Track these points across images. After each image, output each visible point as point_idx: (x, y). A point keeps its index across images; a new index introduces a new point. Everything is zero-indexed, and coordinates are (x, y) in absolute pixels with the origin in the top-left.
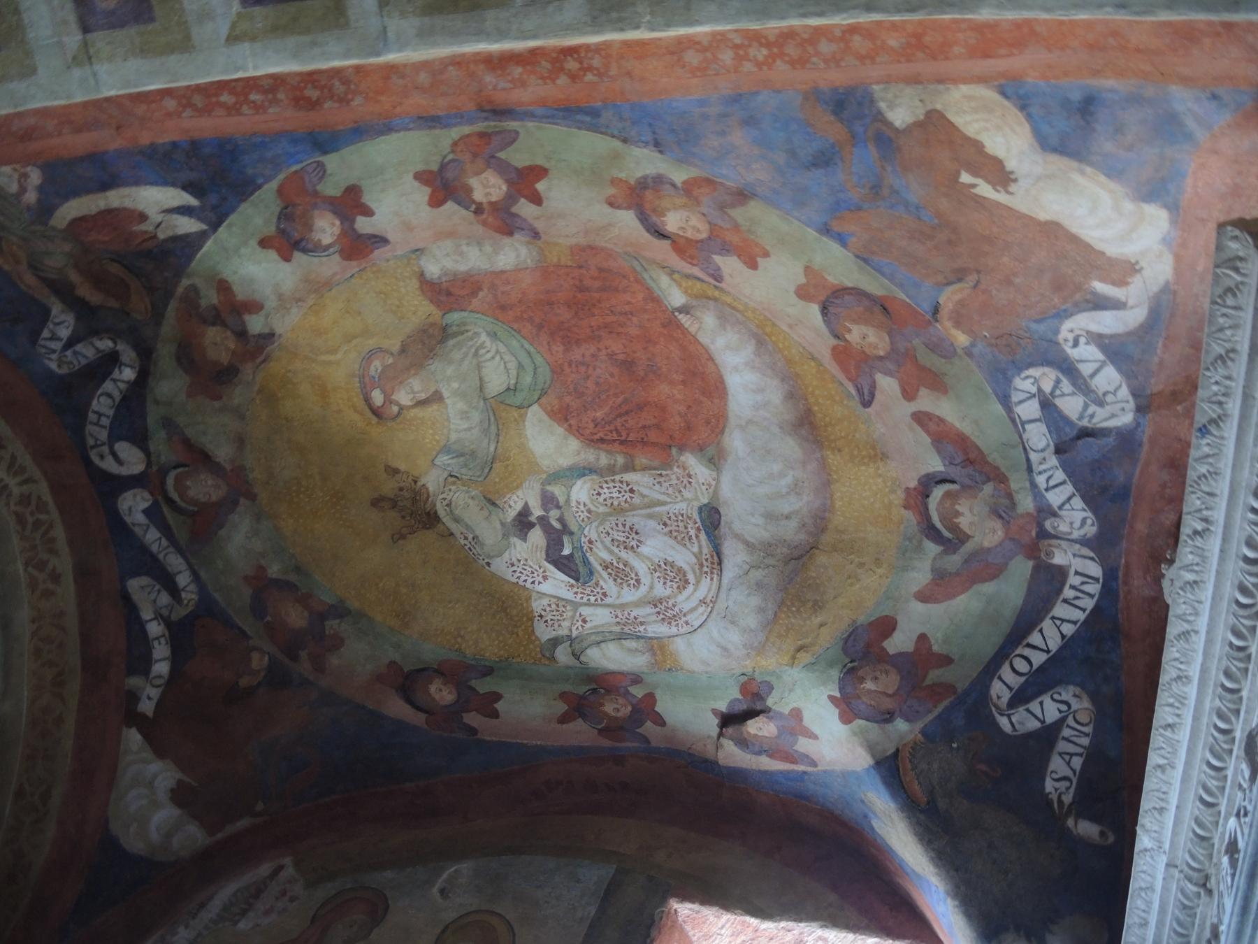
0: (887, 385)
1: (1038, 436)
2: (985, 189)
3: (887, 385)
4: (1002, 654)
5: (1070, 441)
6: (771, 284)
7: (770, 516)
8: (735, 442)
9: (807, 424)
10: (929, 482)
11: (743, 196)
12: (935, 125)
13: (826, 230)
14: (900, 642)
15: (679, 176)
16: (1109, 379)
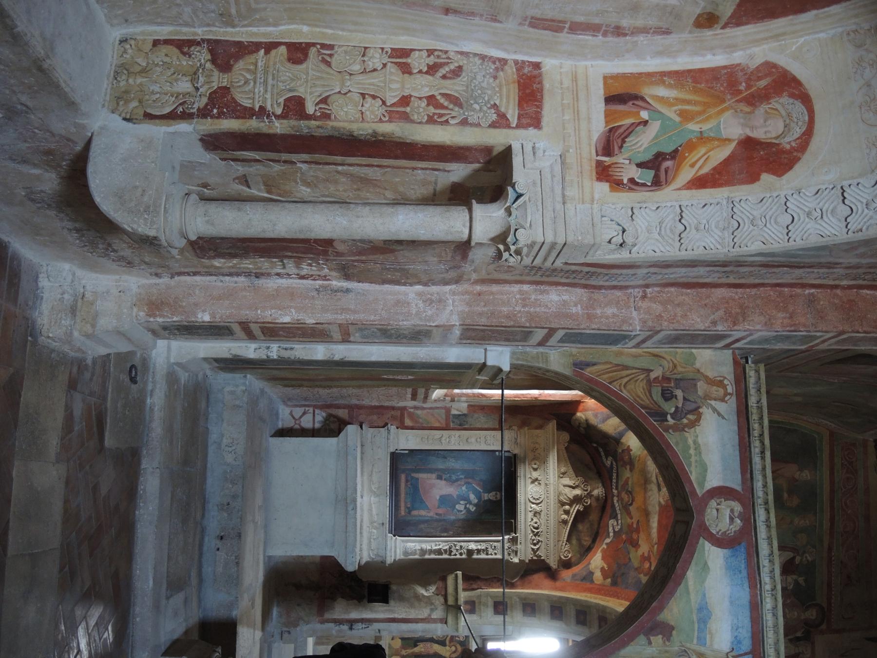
0: (635, 526)
1: (619, 516)
2: (605, 566)
3: (635, 526)
4: (617, 470)
5: (615, 517)
6: (644, 548)
7: (651, 490)
8: (657, 508)
9: (647, 514)
10: (631, 504)
11: (636, 569)
12: (605, 577)
13: (630, 559)
14: (628, 467)
15: (642, 575)
16: (611, 529)
